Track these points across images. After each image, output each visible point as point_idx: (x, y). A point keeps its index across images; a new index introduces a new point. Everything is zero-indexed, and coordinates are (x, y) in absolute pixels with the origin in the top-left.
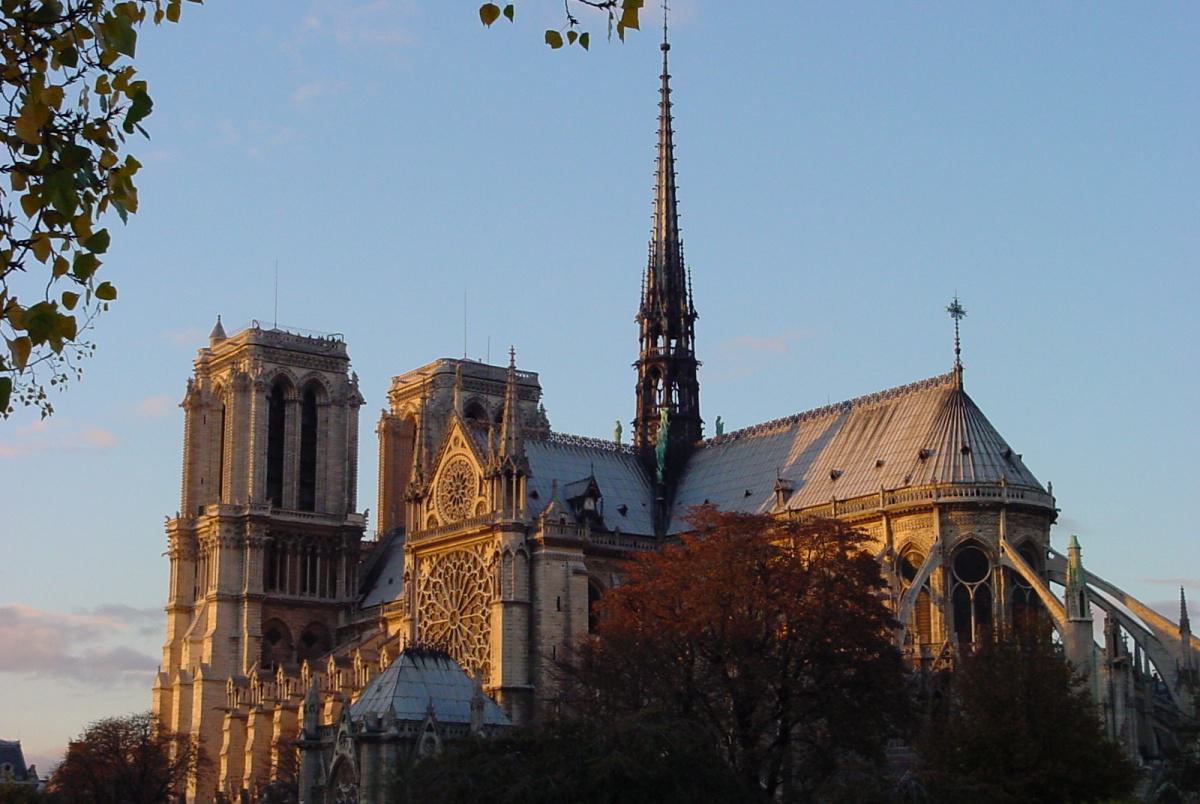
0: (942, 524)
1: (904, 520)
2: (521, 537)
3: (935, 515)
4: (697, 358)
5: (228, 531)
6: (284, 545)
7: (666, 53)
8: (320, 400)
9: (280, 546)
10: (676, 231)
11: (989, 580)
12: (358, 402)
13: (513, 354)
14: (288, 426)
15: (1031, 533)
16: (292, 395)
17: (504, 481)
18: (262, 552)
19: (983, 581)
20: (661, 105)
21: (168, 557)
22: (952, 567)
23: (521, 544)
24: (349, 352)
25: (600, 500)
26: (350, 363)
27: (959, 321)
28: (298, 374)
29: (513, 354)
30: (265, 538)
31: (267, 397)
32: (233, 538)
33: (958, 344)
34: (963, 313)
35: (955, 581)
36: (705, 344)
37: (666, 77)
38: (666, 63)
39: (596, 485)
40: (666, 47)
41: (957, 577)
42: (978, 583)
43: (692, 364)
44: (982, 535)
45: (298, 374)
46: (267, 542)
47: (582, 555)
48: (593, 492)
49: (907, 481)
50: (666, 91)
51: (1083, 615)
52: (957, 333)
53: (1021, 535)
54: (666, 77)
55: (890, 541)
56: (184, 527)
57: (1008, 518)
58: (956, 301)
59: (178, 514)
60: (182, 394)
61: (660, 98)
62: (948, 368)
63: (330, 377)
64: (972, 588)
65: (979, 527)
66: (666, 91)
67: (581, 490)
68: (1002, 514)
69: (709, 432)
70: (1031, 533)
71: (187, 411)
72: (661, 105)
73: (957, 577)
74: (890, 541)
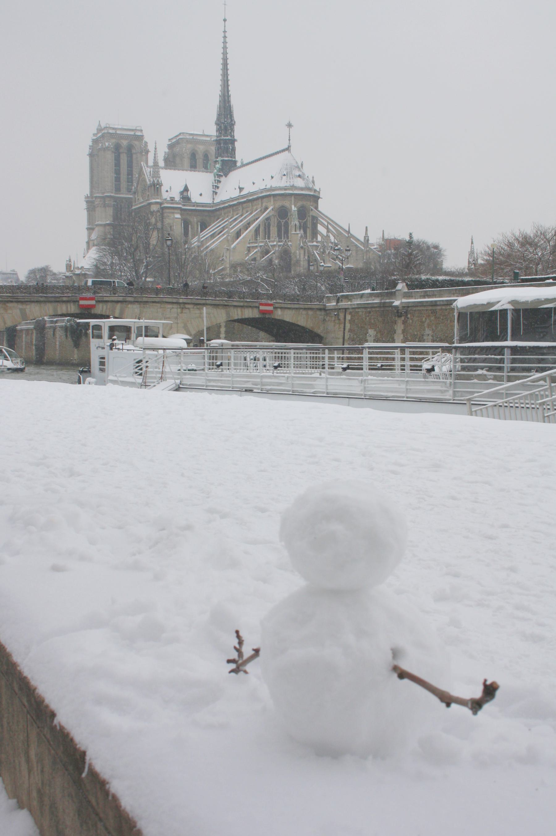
0: (274, 201)
1: (265, 200)
2: (158, 206)
3: (272, 197)
4: (236, 138)
5: (100, 201)
6: (121, 206)
7: (225, 22)
8: (134, 151)
9: (119, 206)
10: (228, 91)
11: (288, 219)
12: (147, 152)
13: (156, 144)
14: (122, 161)
15: (305, 203)
16: (121, 151)
17: (153, 187)
18: (112, 209)
19: (287, 219)
20: (223, 43)
21: (86, 210)
22: (277, 216)
23: (158, 209)
24: (145, 133)
25: (189, 192)
26: (144, 137)
27: (291, 129)
28: (125, 143)
29: (156, 144)
30: (113, 203)
31: (113, 152)
32: (102, 204)
33: (289, 137)
34: (292, 126)
35: (278, 220)
36: (239, 132)
37: (225, 32)
38: (225, 26)
39: (187, 187)
40: (225, 20)
41: (278, 218)
42: (284, 220)
43: (233, 141)
44: (286, 203)
45: (125, 143)
46: (114, 205)
47: (179, 211)
48: (186, 189)
49: (266, 186)
50: (225, 37)
51: (296, 231)
52: (289, 133)
53: (300, 204)
54: (225, 32)
55: (262, 206)
56: (90, 200)
57: (294, 198)
58: (289, 122)
59: (87, 195)
60: (87, 151)
61: (222, 40)
62: (287, 147)
63: (137, 143)
64: (283, 221)
65: (285, 202)
66: (225, 37)
67: (182, 189)
68: (293, 197)
69: (239, 164)
70: (305, 203)
71: (90, 157)
72: (223, 43)
73: (278, 218)
74: (262, 206)
